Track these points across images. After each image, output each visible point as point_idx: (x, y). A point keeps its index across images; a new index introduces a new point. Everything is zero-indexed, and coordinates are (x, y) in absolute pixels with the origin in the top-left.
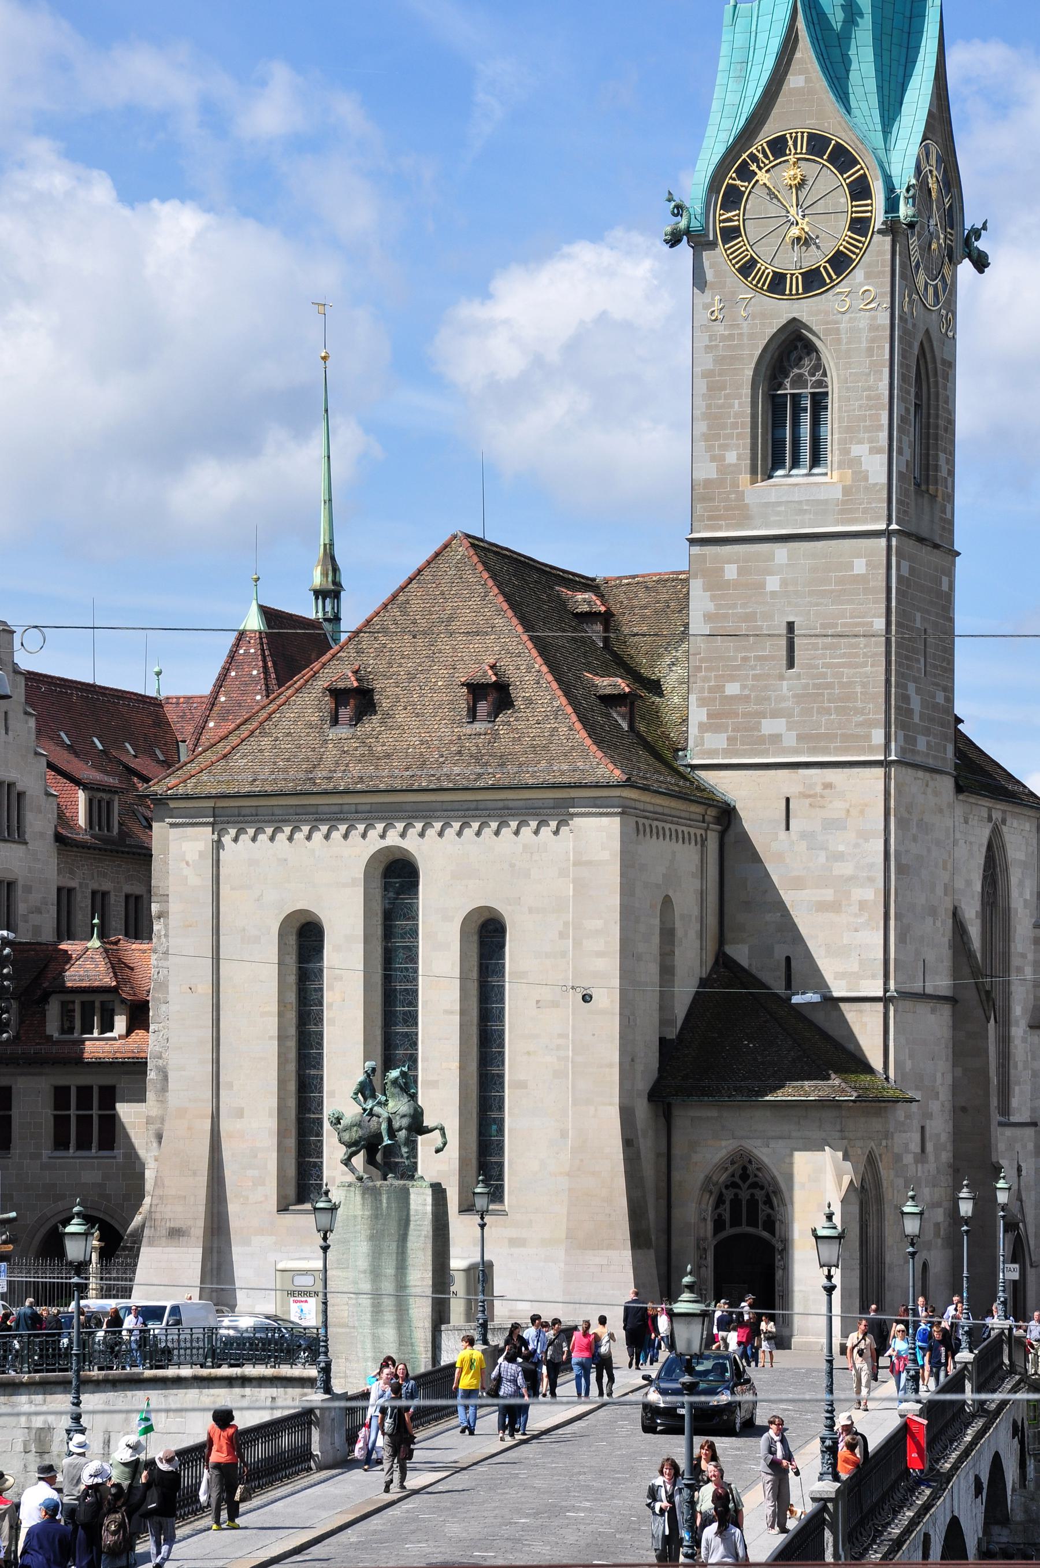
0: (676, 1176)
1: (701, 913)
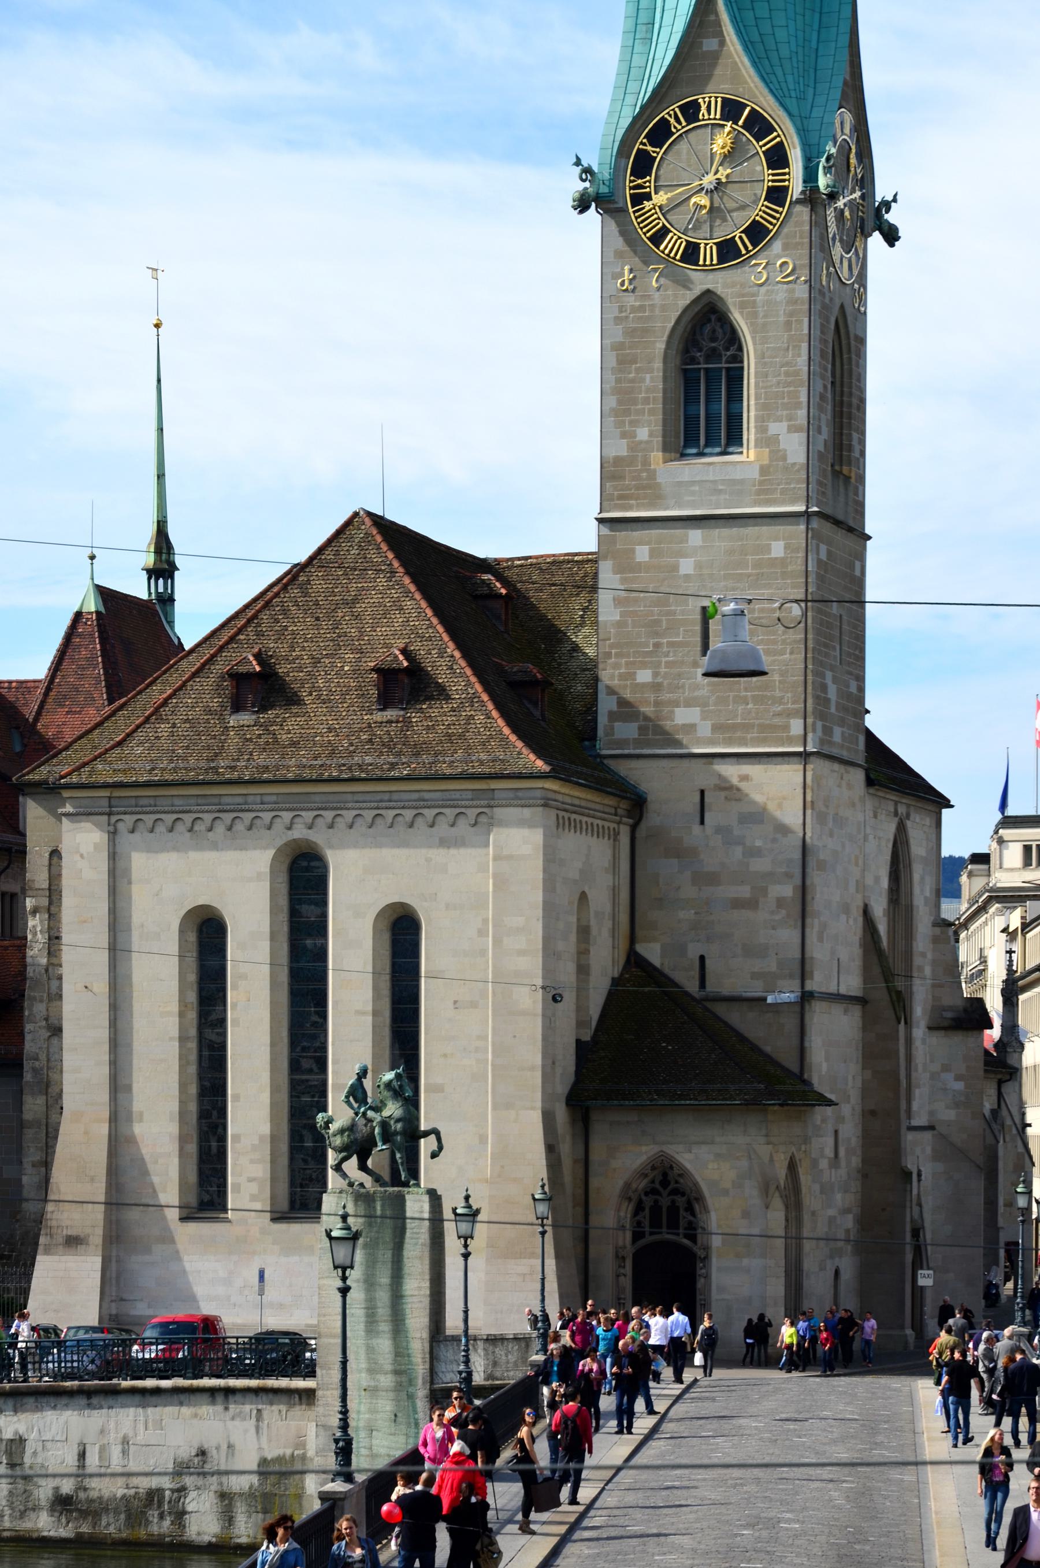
0: (594, 1182)
1: (614, 910)
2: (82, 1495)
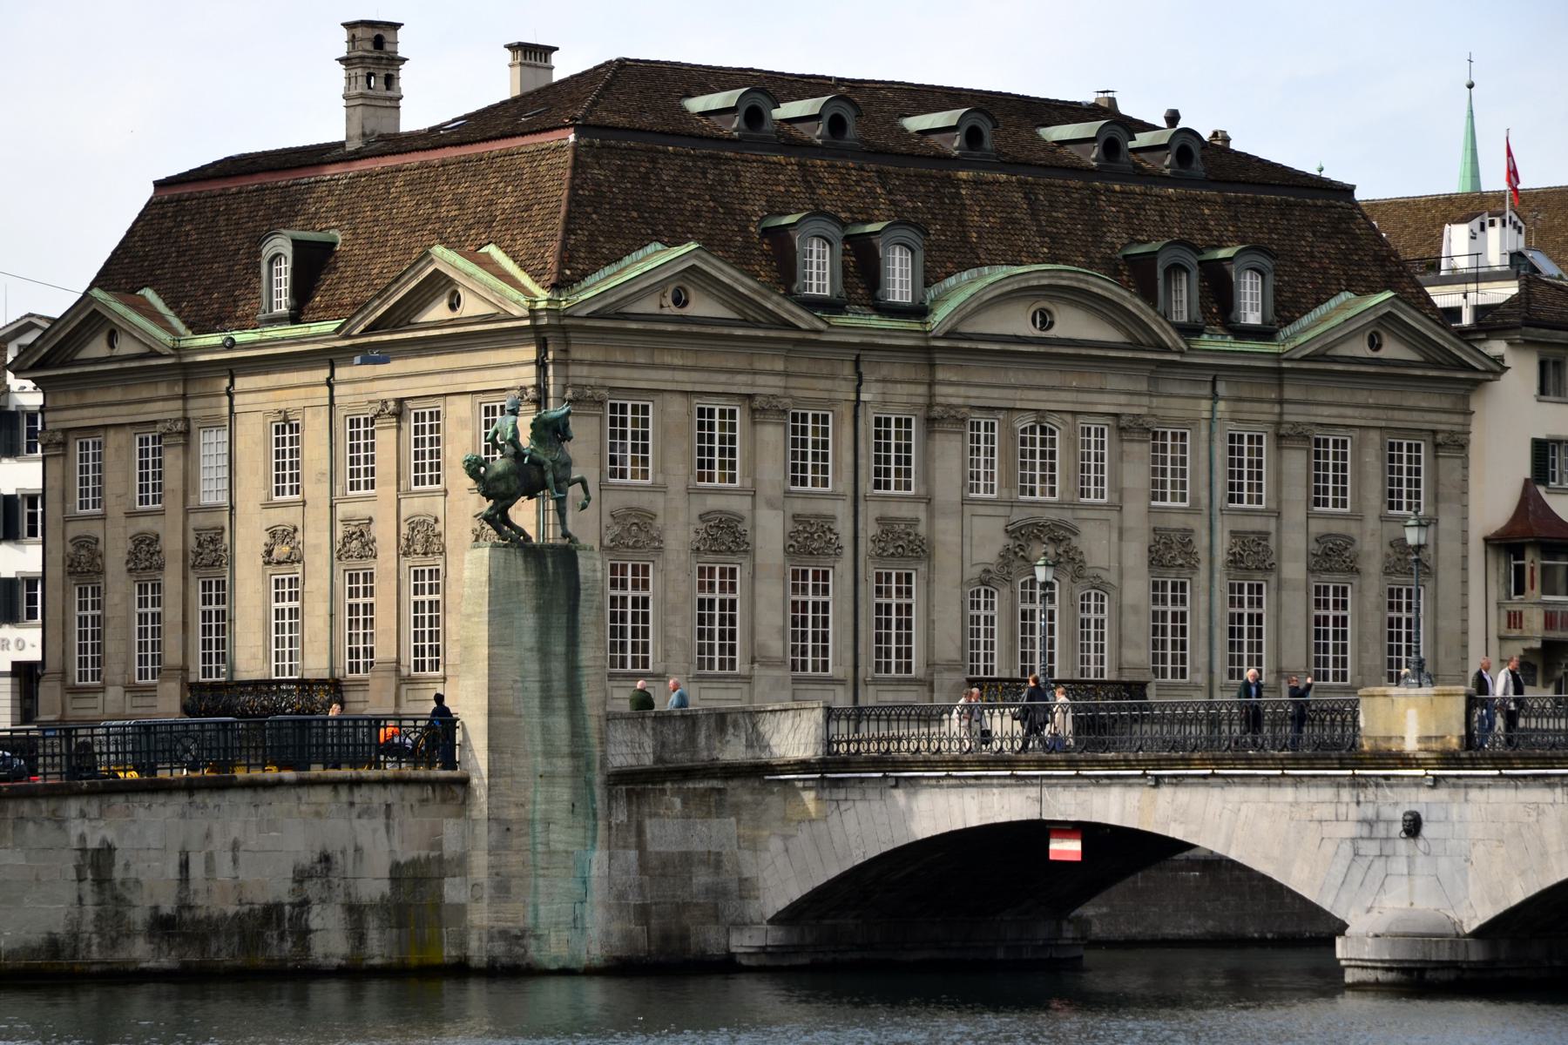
2: (187, 915)
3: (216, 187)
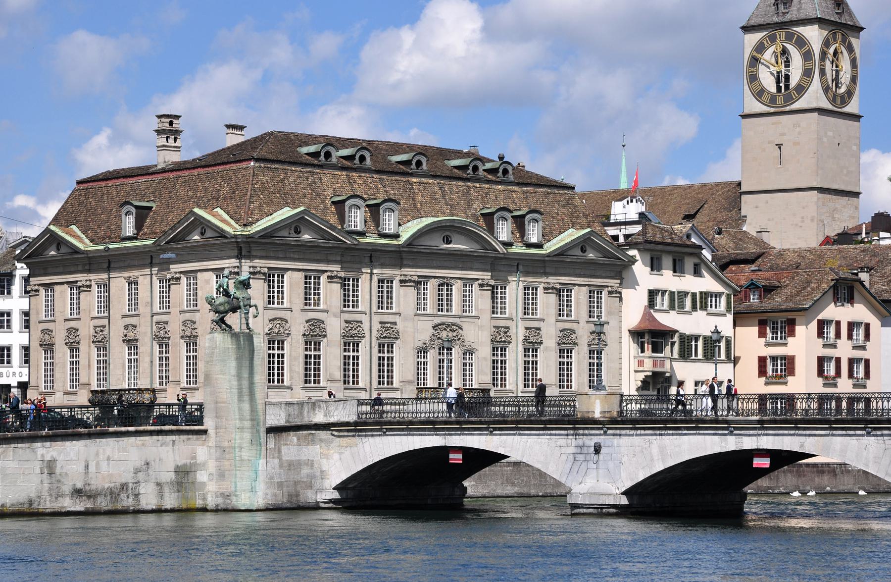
3: (103, 184)
